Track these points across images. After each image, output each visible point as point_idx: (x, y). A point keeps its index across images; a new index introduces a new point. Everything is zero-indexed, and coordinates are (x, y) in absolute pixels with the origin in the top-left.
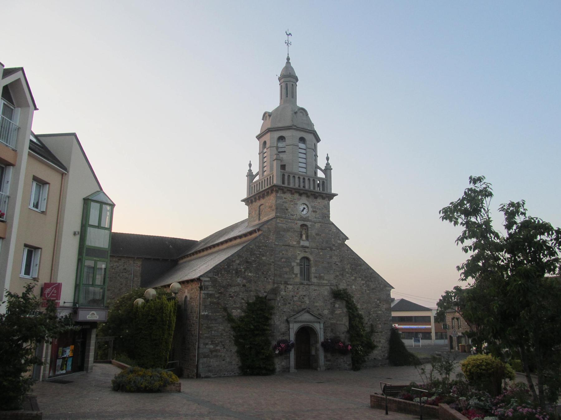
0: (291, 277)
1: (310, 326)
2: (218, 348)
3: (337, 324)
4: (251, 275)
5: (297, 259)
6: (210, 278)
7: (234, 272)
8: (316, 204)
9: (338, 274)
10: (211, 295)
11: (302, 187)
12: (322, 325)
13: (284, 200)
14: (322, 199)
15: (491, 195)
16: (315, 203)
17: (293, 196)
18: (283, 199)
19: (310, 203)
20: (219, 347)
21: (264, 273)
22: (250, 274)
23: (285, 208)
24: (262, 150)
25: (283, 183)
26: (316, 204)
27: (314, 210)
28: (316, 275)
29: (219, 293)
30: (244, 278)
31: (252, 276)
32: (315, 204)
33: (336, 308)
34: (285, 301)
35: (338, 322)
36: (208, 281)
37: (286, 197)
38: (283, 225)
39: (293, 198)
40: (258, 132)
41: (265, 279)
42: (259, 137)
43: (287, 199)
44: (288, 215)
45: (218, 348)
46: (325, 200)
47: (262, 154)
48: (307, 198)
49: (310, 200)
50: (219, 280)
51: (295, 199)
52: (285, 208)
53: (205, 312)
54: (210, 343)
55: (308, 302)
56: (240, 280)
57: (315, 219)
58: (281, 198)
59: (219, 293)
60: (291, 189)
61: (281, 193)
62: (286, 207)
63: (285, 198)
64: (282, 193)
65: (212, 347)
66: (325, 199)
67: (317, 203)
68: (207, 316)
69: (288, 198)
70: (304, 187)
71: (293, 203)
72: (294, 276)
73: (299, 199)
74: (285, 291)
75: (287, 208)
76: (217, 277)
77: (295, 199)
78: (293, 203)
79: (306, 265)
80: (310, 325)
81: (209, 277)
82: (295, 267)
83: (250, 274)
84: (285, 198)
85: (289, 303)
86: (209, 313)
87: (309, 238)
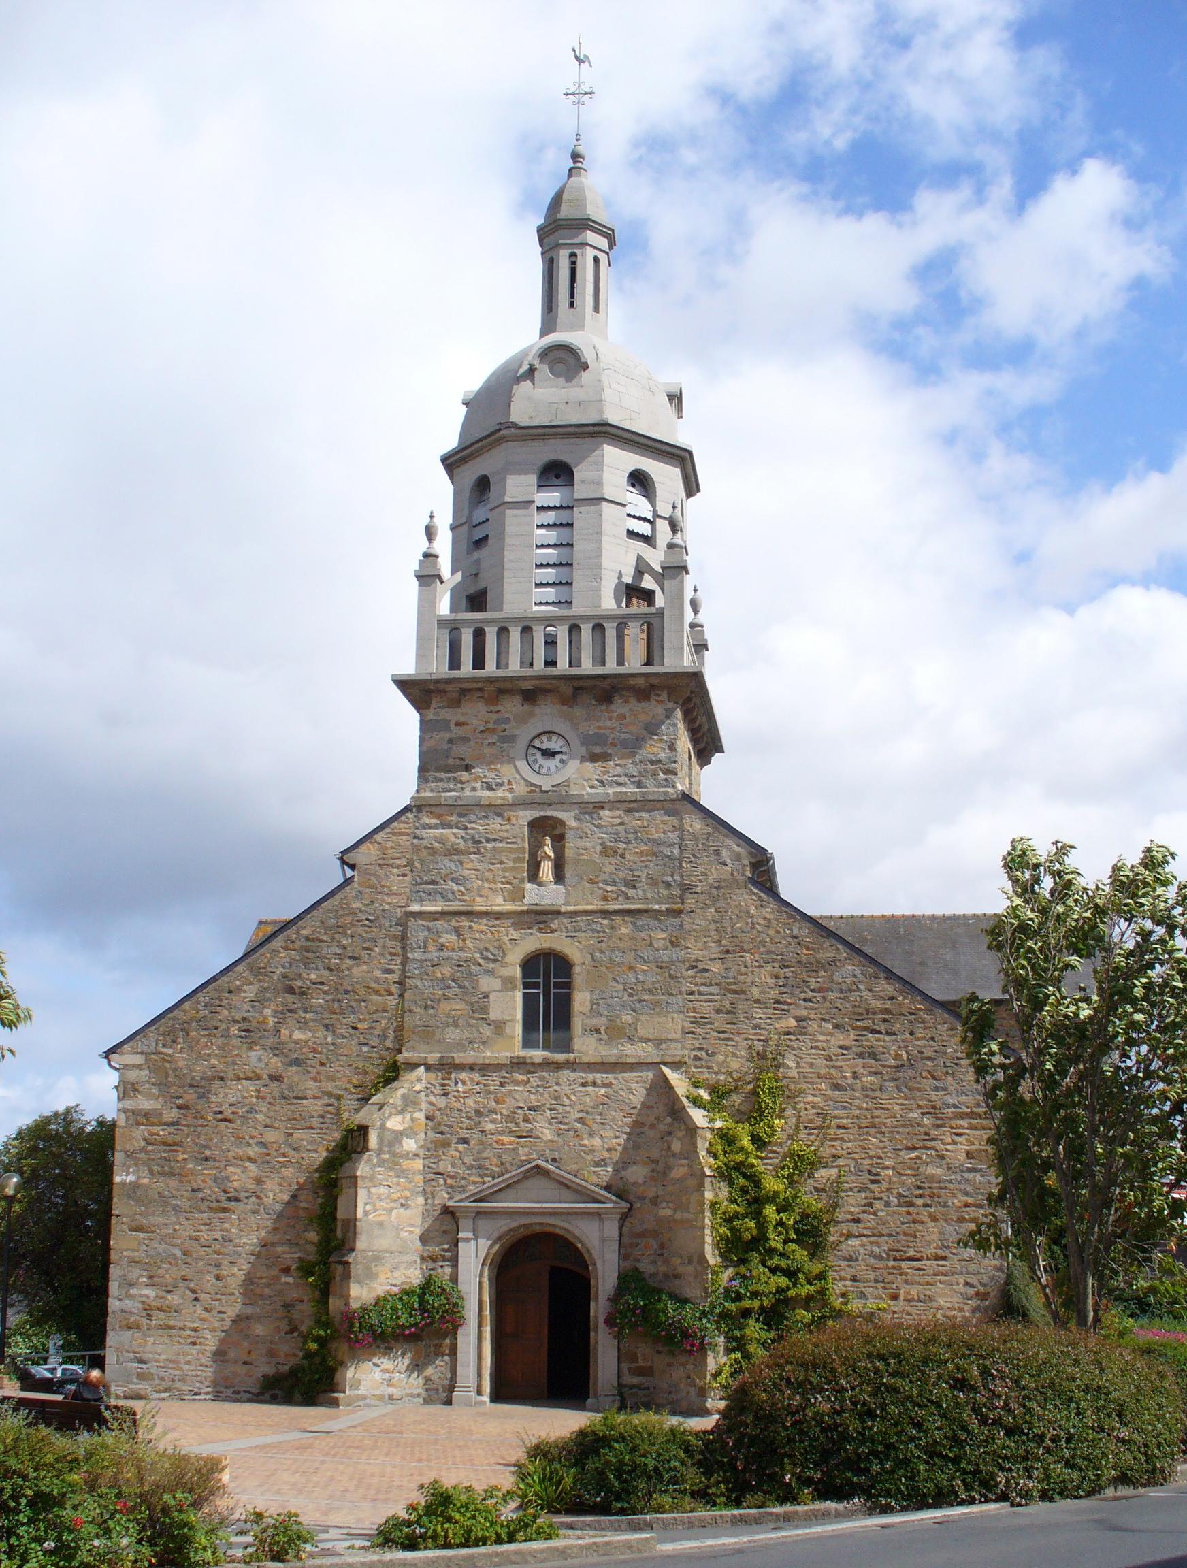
0: (476, 1035)
1: (557, 1231)
2: (174, 1299)
3: (675, 1221)
4: (303, 1037)
5: (504, 965)
6: (144, 1056)
7: (234, 1030)
8: (609, 723)
9: (707, 1009)
10: (147, 1115)
11: (539, 664)
12: (612, 1229)
13: (457, 732)
14: (639, 701)
15: (405, 685)
16: (600, 724)
17: (495, 709)
18: (451, 731)
19: (575, 726)
20: (176, 1297)
21: (359, 1026)
22: (297, 1035)
23: (458, 762)
24: (466, 512)
25: (454, 663)
26: (609, 723)
27: (597, 750)
28: (594, 1022)
29: (180, 1107)
30: (277, 1050)
31: (307, 1042)
32: (599, 728)
33: (674, 1155)
34: (442, 1133)
35: (678, 1216)
36: (139, 1067)
37: (462, 719)
38: (445, 831)
39: (495, 716)
40: (451, 442)
41: (365, 1049)
42: (451, 463)
43: (467, 724)
44: (474, 789)
45: (174, 1299)
46: (653, 702)
47: (465, 528)
48: (565, 708)
49: (578, 711)
50: (182, 1060)
51: (508, 720)
52: (458, 762)
53: (128, 1174)
54: (145, 1280)
55: (548, 1134)
56: (260, 1060)
57: (600, 790)
58: (444, 725)
59: (180, 1107)
60: (479, 685)
61: (443, 707)
62: (463, 759)
63: (458, 724)
64: (445, 703)
65: (150, 1292)
66: (653, 698)
67: (610, 719)
68: (135, 1186)
69: (475, 722)
70: (550, 663)
71: (493, 738)
72: (487, 1031)
73: (522, 720)
74: (446, 1094)
75: (468, 761)
76: (170, 1051)
77: (508, 720)
78: (495, 737)
79: (557, 985)
80: (554, 1226)
81: (142, 1053)
82: (492, 997)
83: (297, 1035)
84: (458, 724)
85: (465, 1141)
86: (139, 1178)
87: (568, 872)
